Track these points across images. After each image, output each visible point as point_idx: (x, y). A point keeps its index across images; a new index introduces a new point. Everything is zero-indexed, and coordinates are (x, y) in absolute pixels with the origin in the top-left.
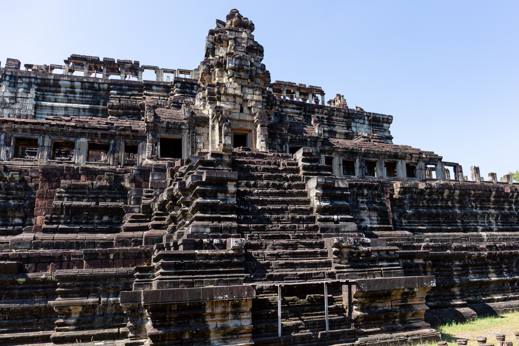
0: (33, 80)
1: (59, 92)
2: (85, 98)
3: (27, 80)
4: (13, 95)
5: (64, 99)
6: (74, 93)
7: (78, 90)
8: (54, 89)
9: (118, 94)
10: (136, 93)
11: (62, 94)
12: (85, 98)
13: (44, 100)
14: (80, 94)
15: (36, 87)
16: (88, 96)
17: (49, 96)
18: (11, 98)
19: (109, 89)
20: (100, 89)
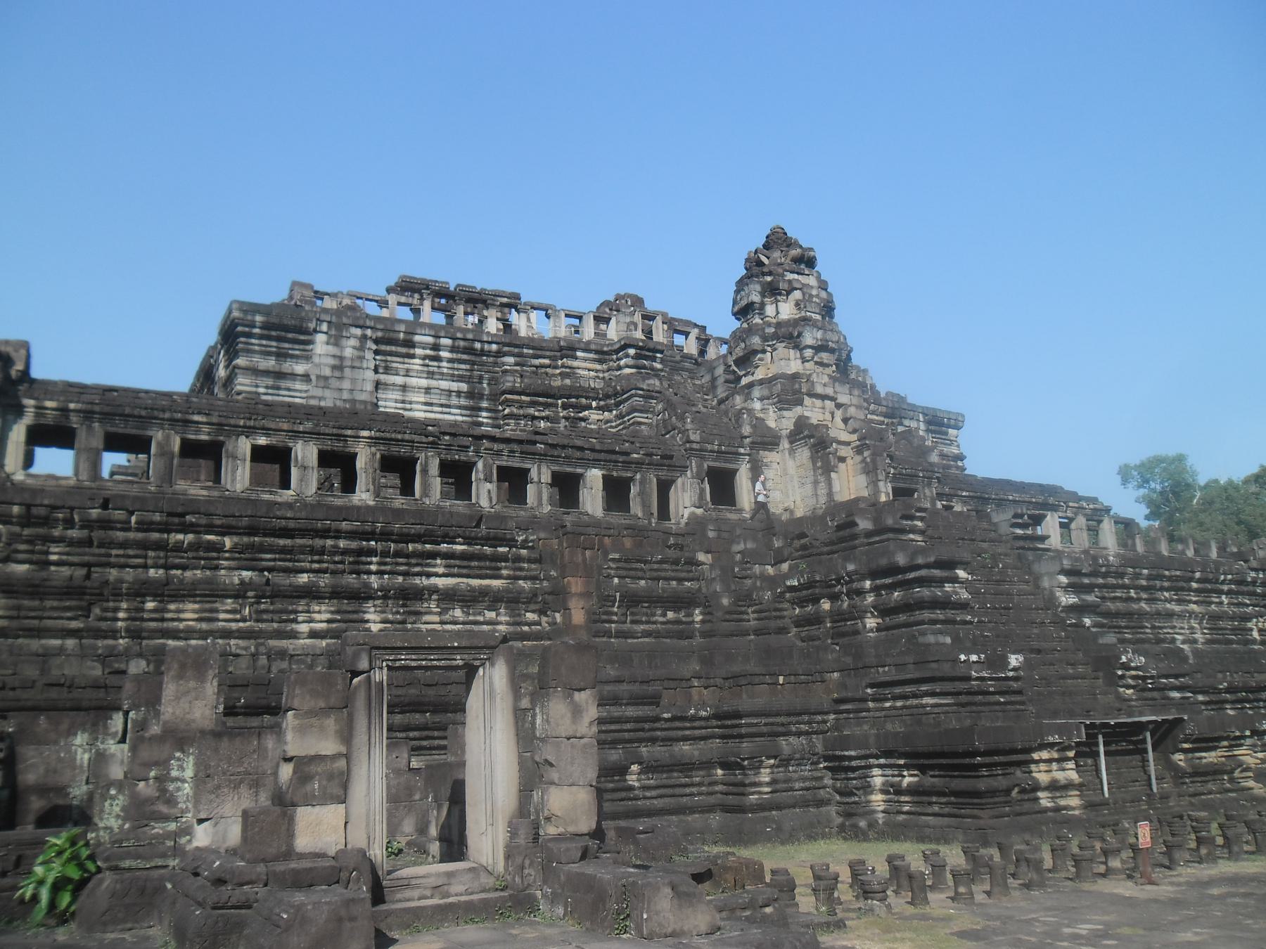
0: (369, 332)
1: (413, 356)
2: (458, 369)
3: (358, 332)
4: (336, 362)
5: (422, 371)
6: (437, 359)
7: (445, 354)
8: (404, 350)
9: (516, 364)
10: (547, 361)
11: (417, 361)
12: (458, 369)
13: (387, 370)
14: (450, 361)
15: (374, 347)
16: (463, 366)
17: (396, 363)
18: (334, 367)
19: (499, 354)
20: (483, 353)
